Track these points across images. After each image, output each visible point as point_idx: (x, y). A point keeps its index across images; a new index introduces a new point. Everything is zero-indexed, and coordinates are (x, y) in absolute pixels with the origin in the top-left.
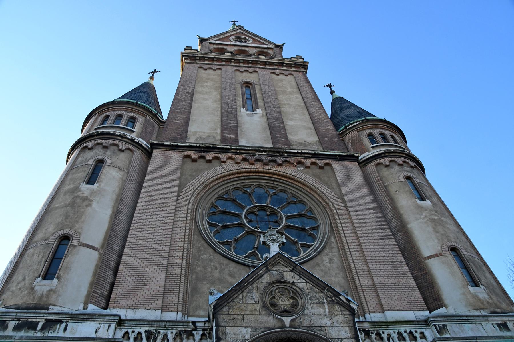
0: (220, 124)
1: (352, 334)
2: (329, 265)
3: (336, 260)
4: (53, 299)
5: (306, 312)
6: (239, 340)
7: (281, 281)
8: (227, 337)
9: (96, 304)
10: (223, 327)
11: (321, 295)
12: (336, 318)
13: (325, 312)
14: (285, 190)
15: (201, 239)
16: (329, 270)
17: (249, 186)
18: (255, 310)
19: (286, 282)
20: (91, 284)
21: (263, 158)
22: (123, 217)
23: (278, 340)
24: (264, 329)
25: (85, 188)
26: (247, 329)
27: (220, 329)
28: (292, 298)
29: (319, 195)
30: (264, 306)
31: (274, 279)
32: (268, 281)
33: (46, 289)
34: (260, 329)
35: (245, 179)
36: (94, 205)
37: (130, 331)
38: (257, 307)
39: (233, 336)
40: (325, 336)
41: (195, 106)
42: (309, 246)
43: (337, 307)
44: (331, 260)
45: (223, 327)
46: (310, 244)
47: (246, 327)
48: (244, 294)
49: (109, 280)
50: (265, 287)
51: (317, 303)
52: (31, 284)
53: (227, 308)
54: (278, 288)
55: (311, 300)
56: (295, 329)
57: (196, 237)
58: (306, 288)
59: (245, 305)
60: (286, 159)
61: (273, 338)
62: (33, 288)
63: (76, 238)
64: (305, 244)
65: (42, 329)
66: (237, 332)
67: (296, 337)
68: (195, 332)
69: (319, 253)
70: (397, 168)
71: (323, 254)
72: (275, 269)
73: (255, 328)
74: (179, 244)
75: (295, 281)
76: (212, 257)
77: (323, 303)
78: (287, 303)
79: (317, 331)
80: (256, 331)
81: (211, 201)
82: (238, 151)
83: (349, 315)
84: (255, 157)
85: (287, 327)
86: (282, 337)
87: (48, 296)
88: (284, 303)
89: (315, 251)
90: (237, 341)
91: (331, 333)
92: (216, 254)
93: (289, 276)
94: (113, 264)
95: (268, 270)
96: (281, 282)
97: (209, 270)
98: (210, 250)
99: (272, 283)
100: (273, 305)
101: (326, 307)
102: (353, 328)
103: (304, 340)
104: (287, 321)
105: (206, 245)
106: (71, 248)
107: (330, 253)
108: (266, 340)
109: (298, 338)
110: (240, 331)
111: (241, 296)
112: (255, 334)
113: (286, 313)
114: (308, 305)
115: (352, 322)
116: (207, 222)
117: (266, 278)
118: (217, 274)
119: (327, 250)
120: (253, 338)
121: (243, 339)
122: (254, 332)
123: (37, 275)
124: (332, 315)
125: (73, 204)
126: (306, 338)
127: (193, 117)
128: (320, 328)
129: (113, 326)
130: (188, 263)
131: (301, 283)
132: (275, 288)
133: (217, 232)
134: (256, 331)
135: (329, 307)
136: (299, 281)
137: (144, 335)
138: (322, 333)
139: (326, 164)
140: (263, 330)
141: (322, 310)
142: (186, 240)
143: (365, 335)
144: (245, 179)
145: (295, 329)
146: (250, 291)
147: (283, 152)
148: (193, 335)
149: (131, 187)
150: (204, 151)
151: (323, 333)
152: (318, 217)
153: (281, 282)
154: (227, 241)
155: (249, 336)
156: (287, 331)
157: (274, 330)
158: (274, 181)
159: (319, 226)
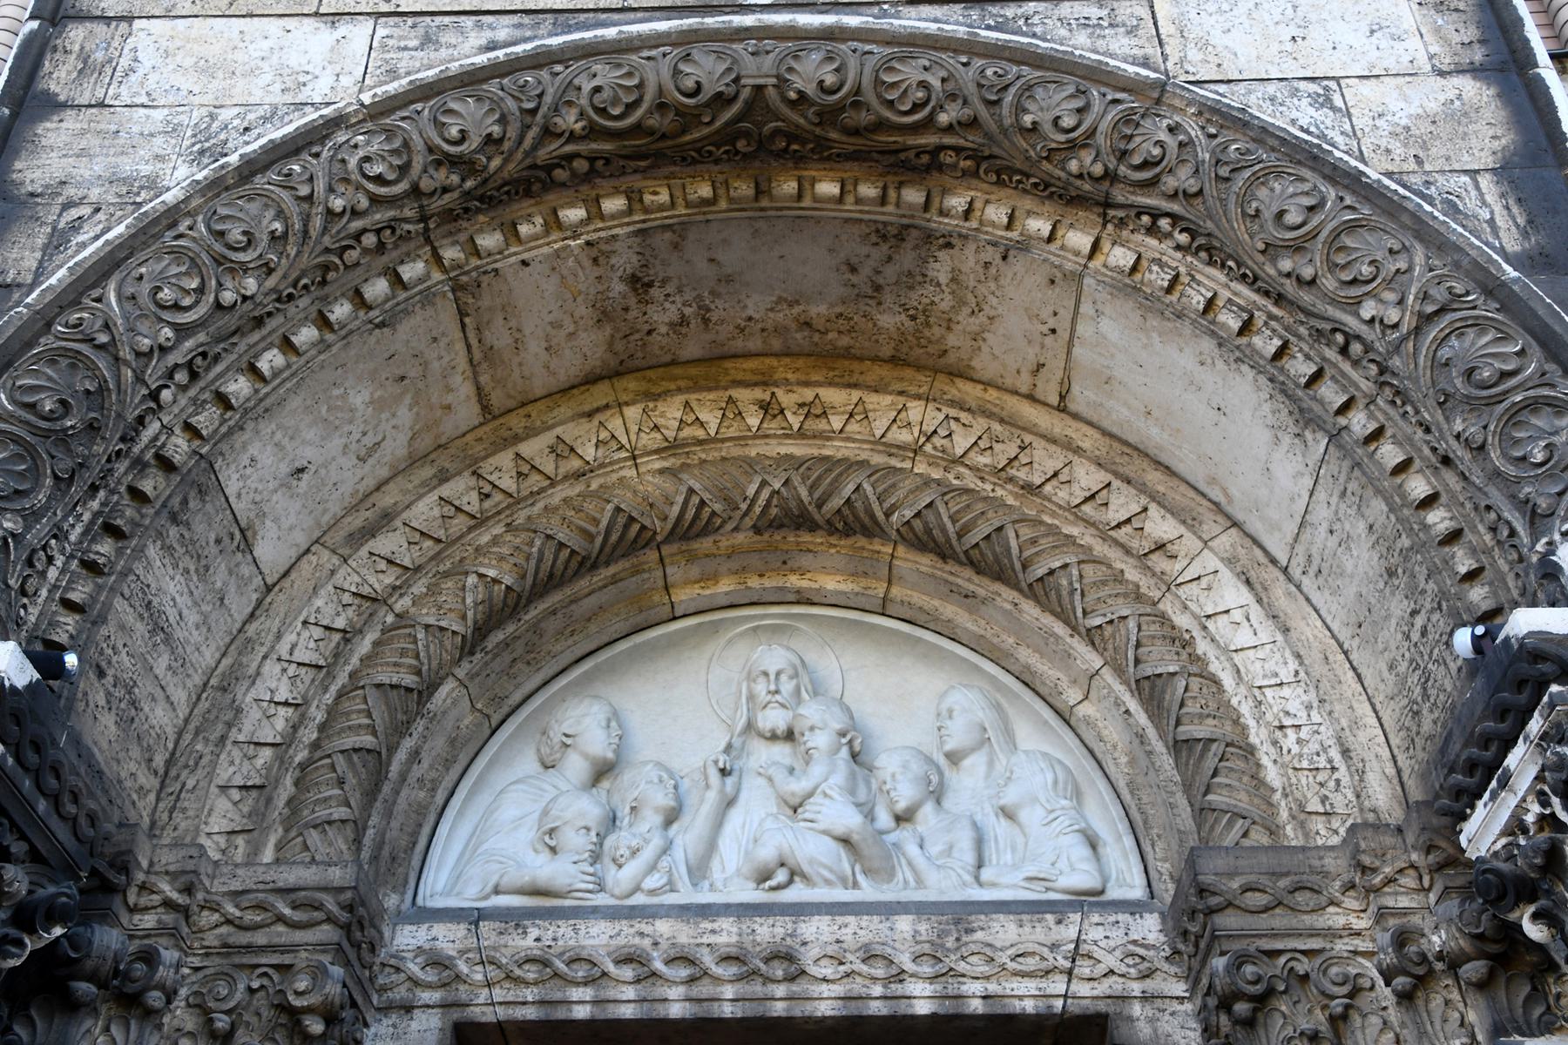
1: (1456, 38)
6: (236, 110)
10: (107, 20)
23: (639, 113)
24: (519, 26)
26: (344, 28)
34: (479, 26)
40: (1145, 63)
45: (107, 20)
47: (336, 17)
56: (829, 19)
61: (587, 87)
66: (240, 56)
67: (830, 80)
79: (1063, 32)
86: (689, 84)
90: (212, 117)
91: (1217, 38)
103: (916, 107)
108: (511, 104)
109: (858, 91)
110: (266, 44)
120: (379, 91)
121: (289, 98)
122: (406, 48)
126: (936, 83)
134: (428, 41)
140: (502, 35)
145: (829, 19)
151: (1125, 41)
155: (346, 81)
156: (742, 34)
157: (611, 33)
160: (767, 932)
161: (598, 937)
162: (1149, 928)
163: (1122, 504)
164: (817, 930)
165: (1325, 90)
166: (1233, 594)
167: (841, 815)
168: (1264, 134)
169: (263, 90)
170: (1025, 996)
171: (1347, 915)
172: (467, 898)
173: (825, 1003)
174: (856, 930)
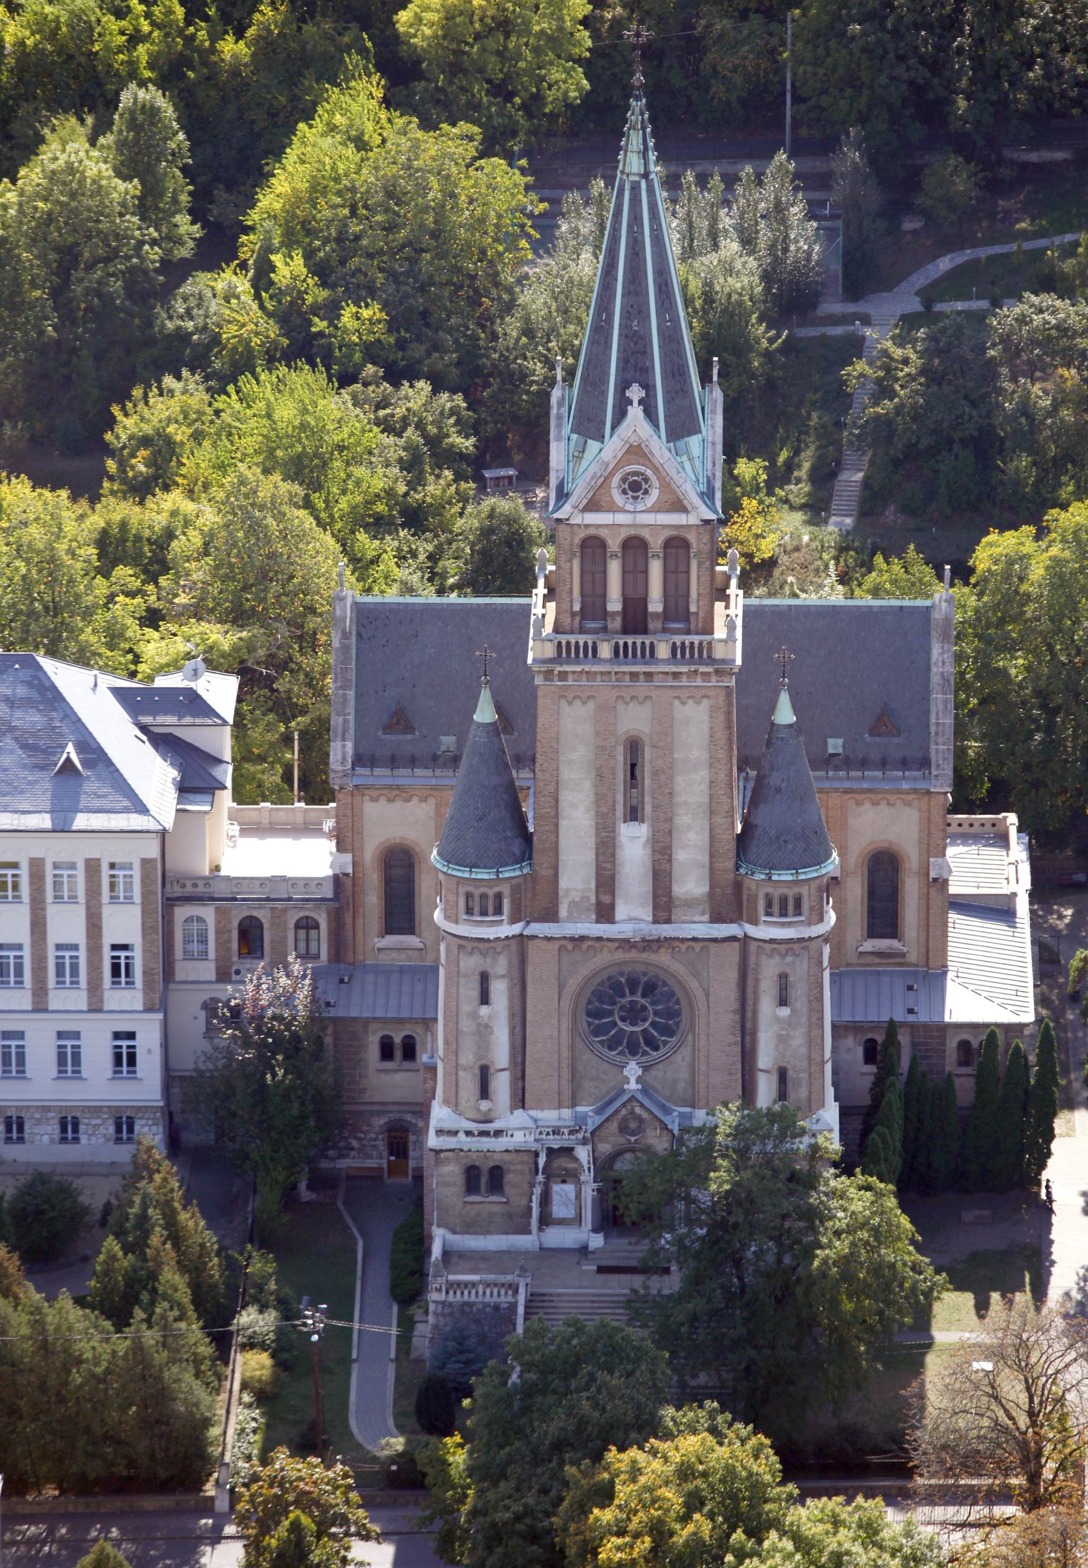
0: (594, 868)
4: (493, 1115)
22: (518, 1030)
25: (484, 1010)
36: (495, 1030)
41: (563, 823)
70: (777, 958)
93: (638, 1110)
113: (633, 1134)
117: (624, 1112)
125: (478, 1033)
127: (562, 857)
149: (517, 990)
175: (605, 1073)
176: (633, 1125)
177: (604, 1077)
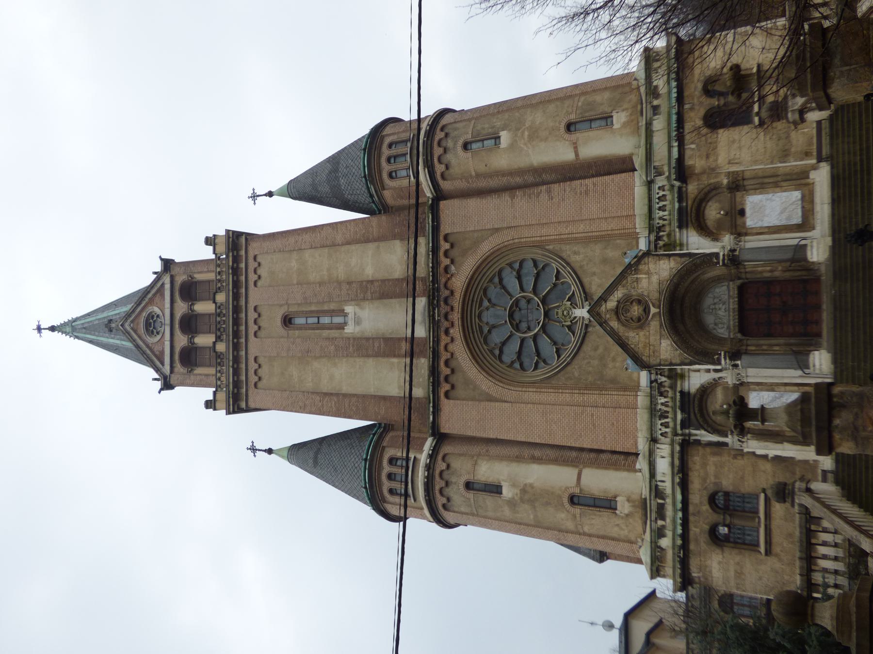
0: (380, 359)
2: (581, 256)
3: (575, 249)
4: (635, 497)
5: (646, 293)
7: (617, 311)
8: (669, 357)
9: (634, 463)
11: (629, 279)
12: (651, 269)
13: (645, 278)
14: (484, 289)
15: (556, 377)
16: (587, 256)
17: (480, 327)
18: (644, 335)
19: (617, 307)
20: (617, 469)
21: (443, 312)
22: (537, 453)
25: (507, 492)
27: (662, 363)
28: (632, 303)
29: (492, 254)
30: (641, 327)
31: (615, 317)
32: (616, 322)
33: (627, 505)
35: (473, 333)
36: (530, 481)
37: (660, 432)
38: (642, 333)
39: (668, 353)
40: (667, 281)
41: (345, 389)
42: (558, 272)
43: (641, 267)
44: (575, 253)
46: (556, 271)
47: (661, 343)
48: (630, 343)
49: (609, 456)
50: (623, 325)
51: (637, 284)
52: (622, 518)
53: (643, 358)
54: (623, 314)
55: (634, 288)
57: (553, 382)
58: (623, 291)
59: (640, 343)
60: (442, 286)
62: (627, 515)
63: (571, 491)
64: (556, 276)
65: (664, 499)
68: (659, 381)
69: (568, 264)
70: (449, 157)
71: (568, 260)
72: (603, 316)
73: (661, 336)
74: (566, 397)
75: (616, 299)
76: (576, 367)
77: (637, 278)
78: (636, 308)
80: (664, 335)
81: (506, 368)
82: (436, 339)
83: (648, 258)
84: (443, 320)
85: (660, 311)
87: (633, 501)
88: (636, 310)
89: (565, 268)
92: (573, 363)
93: (611, 304)
94: (592, 455)
95: (605, 322)
96: (617, 311)
97: (591, 369)
98: (569, 368)
99: (619, 319)
100: (639, 320)
101: (641, 276)
102: (661, 257)
104: (653, 310)
105: (562, 373)
106: (583, 492)
107: (568, 252)
111: (633, 346)
112: (666, 337)
113: (646, 310)
114: (640, 291)
115: (655, 257)
116: (533, 371)
117: (614, 324)
118: (596, 362)
119: (564, 255)
123: (614, 515)
124: (648, 273)
125: (532, 502)
127: (372, 391)
128: (661, 285)
129: (658, 446)
130: (586, 388)
131: (619, 294)
132: (623, 317)
133: (545, 362)
135: (641, 274)
136: (616, 296)
137: (663, 421)
138: (665, 283)
139: (446, 238)
141: (644, 280)
142: (560, 391)
143: (660, 241)
144: (473, 333)
146: (628, 338)
147: (433, 289)
148: (662, 382)
149: (494, 450)
150: (438, 377)
152: (521, 257)
153: (617, 311)
154: (556, 352)
158: (473, 301)
159: (532, 259)
160: (731, 310)
161: (732, 323)
162: (731, 283)
163: (697, 283)
164: (731, 307)
165: (671, 269)
166: (706, 275)
167: (721, 305)
168: (676, 274)
169: (669, 348)
170: (736, 292)
171: (733, 271)
172: (727, 334)
173: (736, 306)
174: (731, 304)
175: (596, 349)
176: (636, 310)
177: (600, 350)
